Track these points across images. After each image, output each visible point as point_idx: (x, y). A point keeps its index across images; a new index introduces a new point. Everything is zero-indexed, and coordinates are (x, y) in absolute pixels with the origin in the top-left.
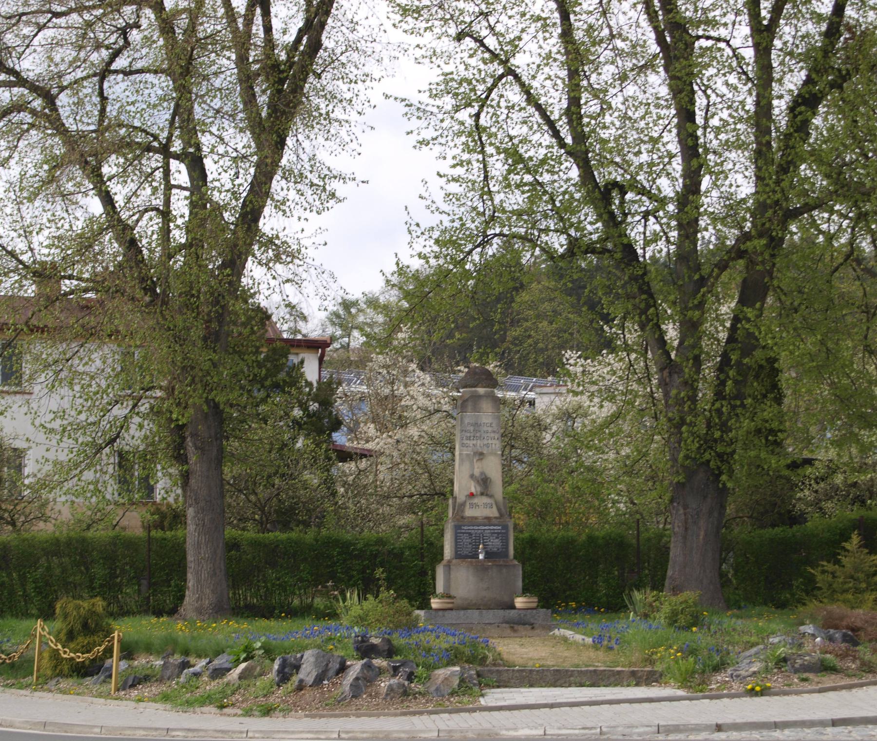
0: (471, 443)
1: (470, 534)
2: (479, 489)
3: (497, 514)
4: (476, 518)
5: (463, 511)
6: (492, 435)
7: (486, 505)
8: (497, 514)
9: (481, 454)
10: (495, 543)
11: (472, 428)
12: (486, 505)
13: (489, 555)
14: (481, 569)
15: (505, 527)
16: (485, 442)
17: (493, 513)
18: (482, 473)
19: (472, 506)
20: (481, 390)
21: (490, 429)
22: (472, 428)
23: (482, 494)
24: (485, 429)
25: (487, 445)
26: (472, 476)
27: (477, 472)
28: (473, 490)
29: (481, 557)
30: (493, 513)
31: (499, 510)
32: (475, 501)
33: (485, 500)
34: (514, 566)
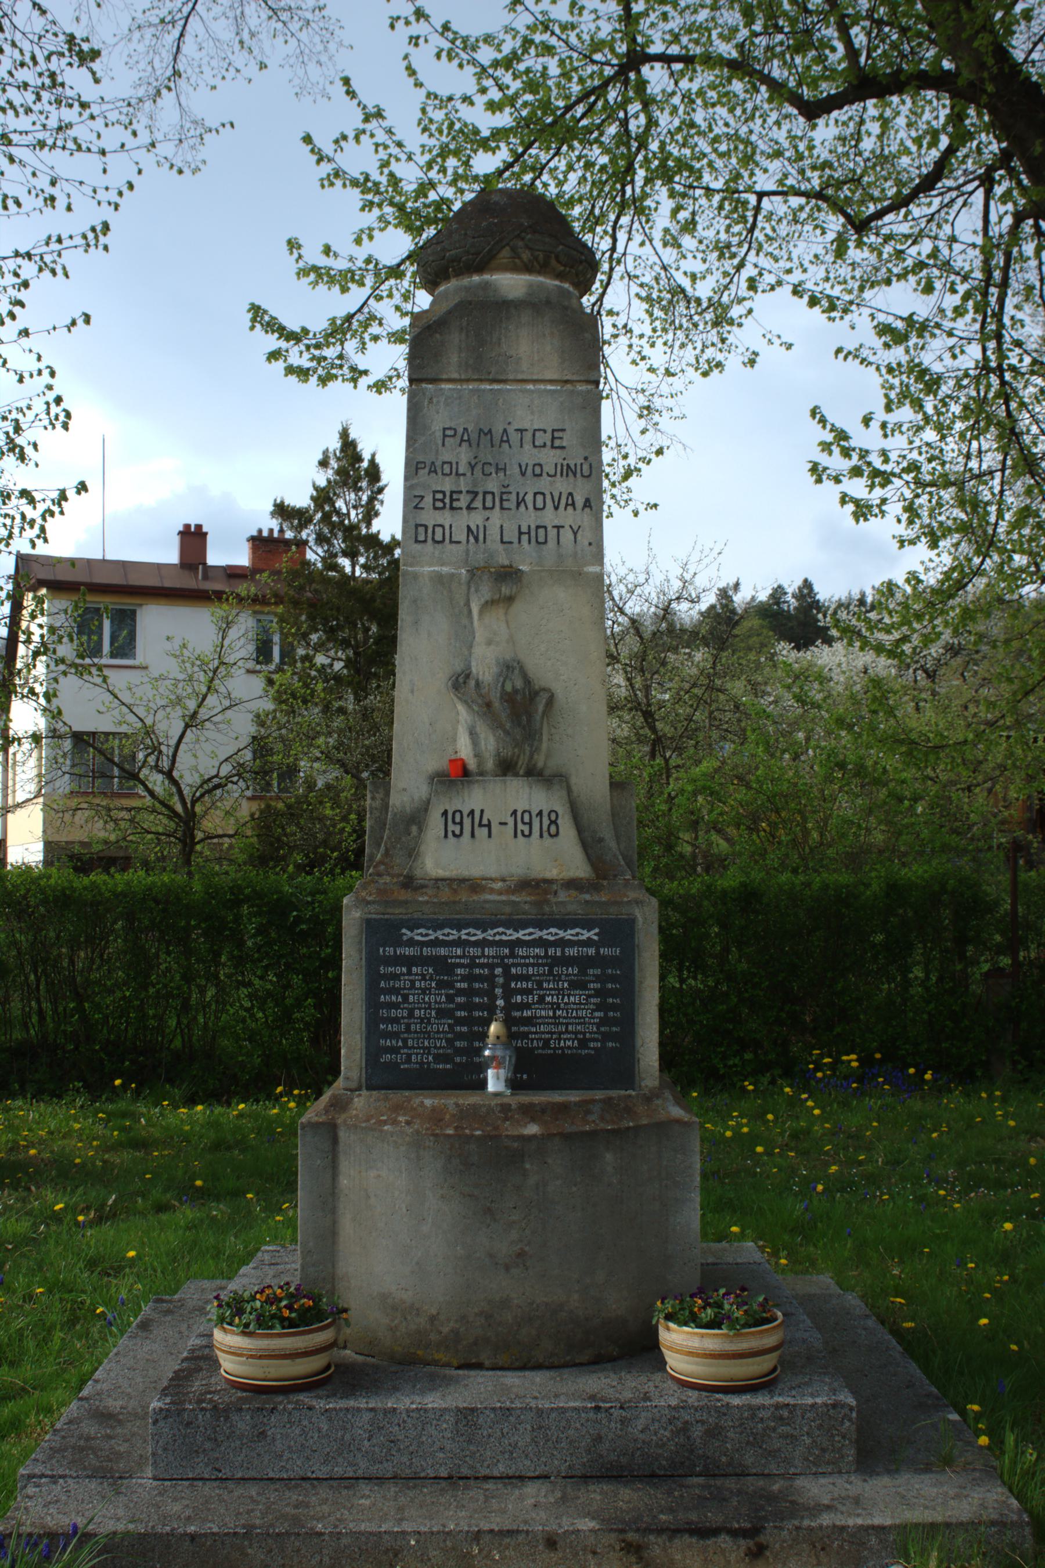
0: (459, 523)
1: (443, 966)
2: (490, 742)
3: (578, 867)
4: (474, 885)
5: (413, 853)
6: (562, 486)
7: (523, 823)
8: (578, 867)
9: (508, 575)
10: (569, 1014)
11: (464, 456)
12: (523, 823)
13: (531, 1070)
14: (483, 1160)
15: (619, 931)
16: (528, 518)
17: (561, 858)
18: (510, 667)
19: (456, 824)
20: (511, 283)
21: (549, 458)
22: (464, 456)
23: (506, 768)
24: (528, 455)
25: (537, 535)
26: (461, 682)
27: (484, 664)
28: (464, 750)
29: (494, 1081)
30: (561, 858)
31: (589, 843)
32: (474, 799)
33: (520, 795)
34: (664, 1128)
